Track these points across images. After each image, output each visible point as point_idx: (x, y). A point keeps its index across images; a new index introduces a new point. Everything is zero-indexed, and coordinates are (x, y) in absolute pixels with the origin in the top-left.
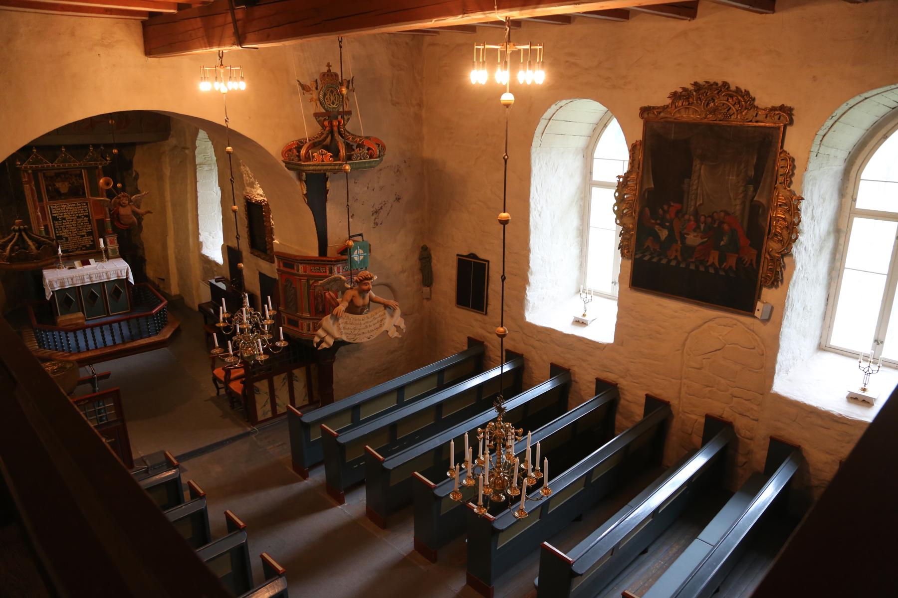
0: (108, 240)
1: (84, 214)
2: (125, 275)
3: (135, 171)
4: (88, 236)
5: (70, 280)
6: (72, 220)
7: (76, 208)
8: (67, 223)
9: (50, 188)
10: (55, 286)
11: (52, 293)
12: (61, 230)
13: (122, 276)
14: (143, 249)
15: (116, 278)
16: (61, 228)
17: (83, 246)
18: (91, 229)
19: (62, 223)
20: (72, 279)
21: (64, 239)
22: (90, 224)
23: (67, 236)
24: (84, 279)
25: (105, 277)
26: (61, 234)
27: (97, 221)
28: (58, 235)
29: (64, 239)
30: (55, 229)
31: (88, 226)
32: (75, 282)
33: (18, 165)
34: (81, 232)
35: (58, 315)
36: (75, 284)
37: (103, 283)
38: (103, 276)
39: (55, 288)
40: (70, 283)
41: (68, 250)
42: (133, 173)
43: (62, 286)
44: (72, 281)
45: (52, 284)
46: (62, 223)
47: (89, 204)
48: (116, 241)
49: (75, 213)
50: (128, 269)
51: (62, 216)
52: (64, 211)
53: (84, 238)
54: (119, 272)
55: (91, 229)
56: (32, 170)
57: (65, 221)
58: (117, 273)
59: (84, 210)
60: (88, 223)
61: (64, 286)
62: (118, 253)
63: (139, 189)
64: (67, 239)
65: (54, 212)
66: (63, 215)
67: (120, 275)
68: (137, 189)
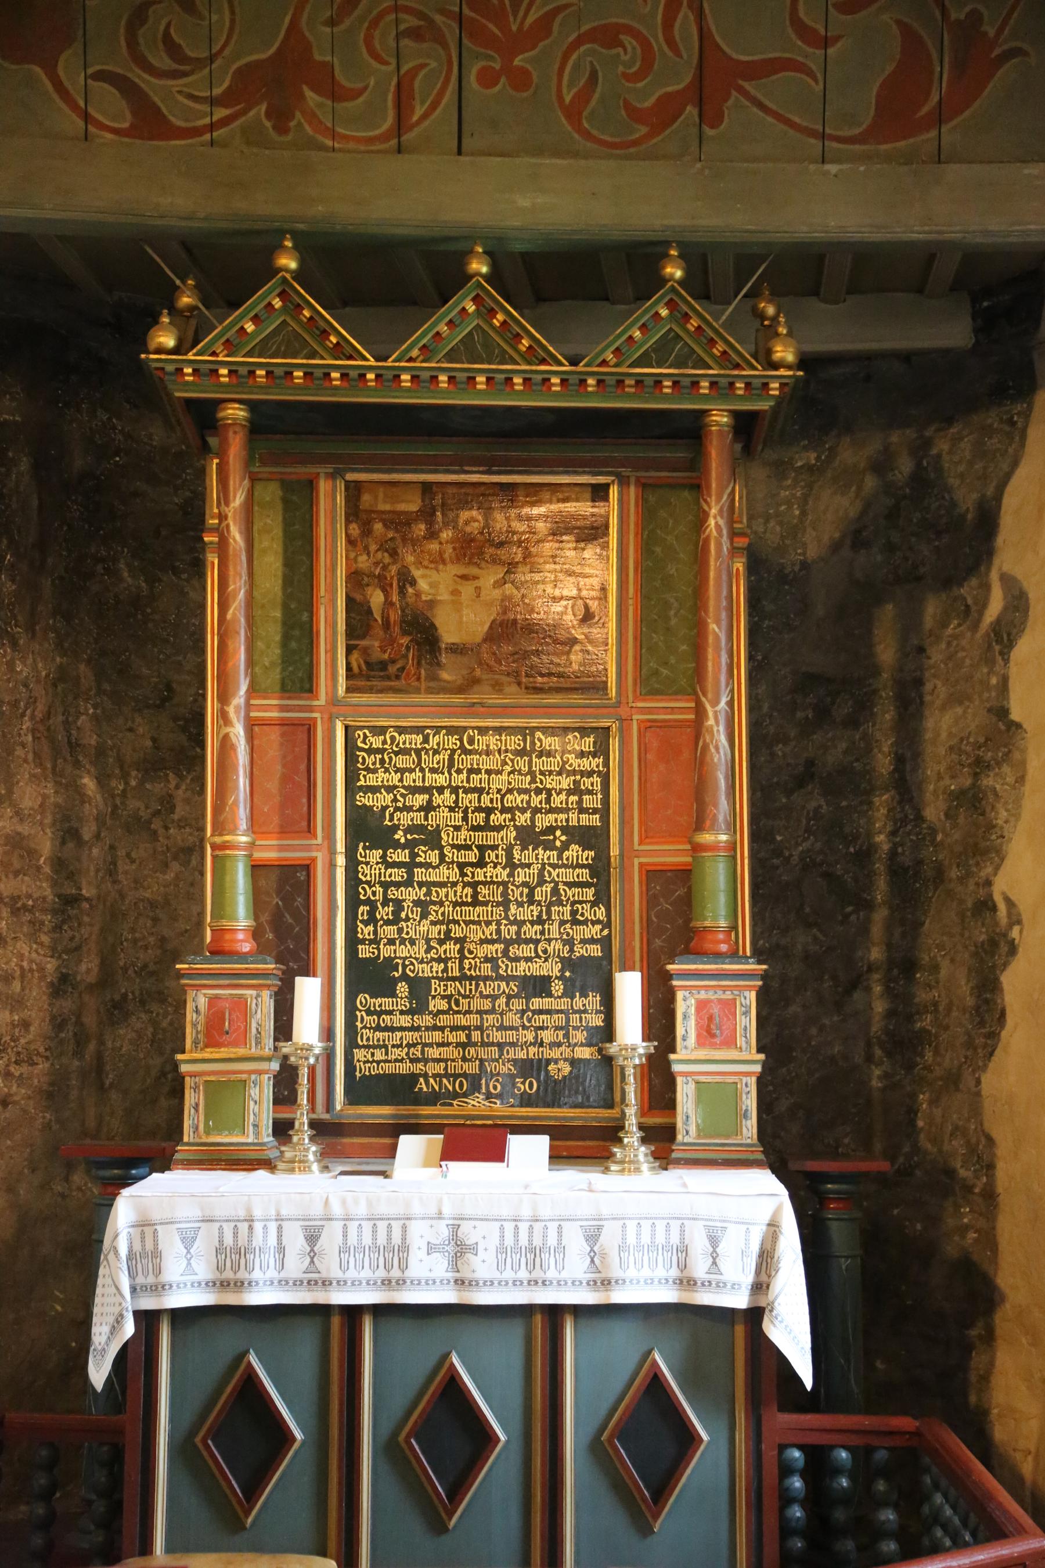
0: (685, 1005)
1: (574, 818)
2: (749, 1279)
3: (1007, 580)
4: (569, 993)
5: (296, 1241)
6: (482, 849)
7: (522, 764)
8: (445, 873)
9: (376, 598)
10: (173, 1269)
11: (129, 1329)
12: (396, 920)
13: (721, 1285)
14: (990, 1195)
15: (668, 1296)
16: (398, 904)
17: (529, 1068)
18: (606, 943)
19: (410, 866)
20: (312, 1238)
21: (402, 988)
22: (602, 898)
23: (425, 971)
24: (404, 1248)
25: (577, 1266)
26: (386, 951)
27: (651, 874)
28: (365, 952)
29: (402, 988)
30: (353, 902)
31: (586, 911)
32: (330, 1267)
33: (159, 351)
34: (527, 950)
35: (146, 1549)
36: (326, 1283)
37: (554, 1313)
38: (561, 1248)
39: (159, 1289)
40: (295, 1266)
41: (413, 1078)
42: (983, 605)
43: (224, 1285)
44: (312, 1255)
45: (156, 1254)
46: (410, 866)
47: (614, 745)
48: (747, 1023)
49: (510, 800)
50: (773, 1227)
51: (418, 818)
52: (441, 780)
53: (537, 1003)
54: (699, 1245)
55: (606, 943)
56: (252, 406)
57: (433, 857)
58: (684, 1250)
59: (575, 790)
60: (590, 893)
61: (239, 1285)
62: (750, 1129)
63: (1015, 715)
64: (420, 989)
65: (372, 780)
66: (428, 808)
67: (700, 1269)
68: (1003, 713)
